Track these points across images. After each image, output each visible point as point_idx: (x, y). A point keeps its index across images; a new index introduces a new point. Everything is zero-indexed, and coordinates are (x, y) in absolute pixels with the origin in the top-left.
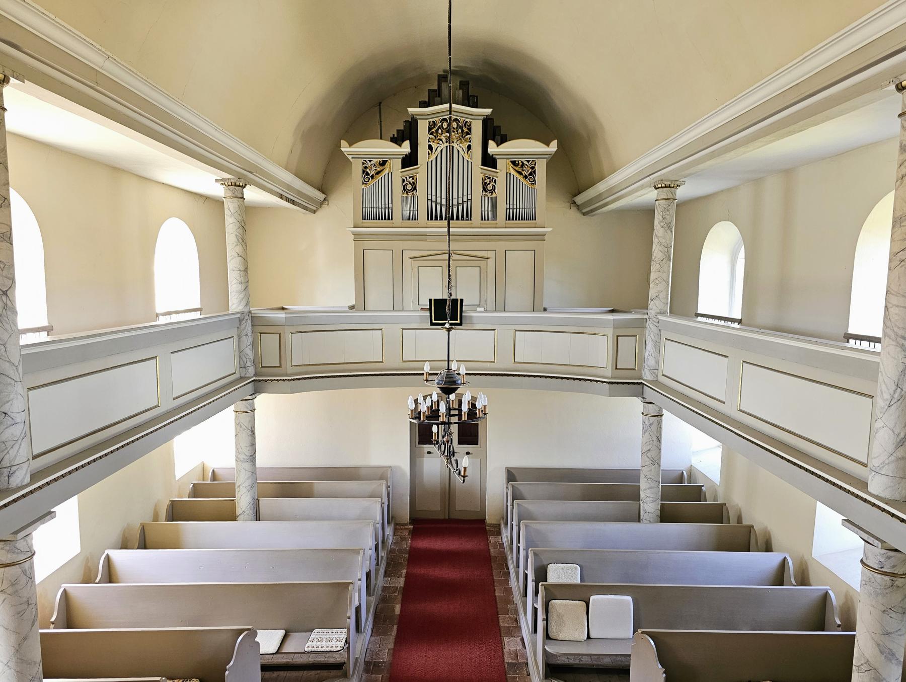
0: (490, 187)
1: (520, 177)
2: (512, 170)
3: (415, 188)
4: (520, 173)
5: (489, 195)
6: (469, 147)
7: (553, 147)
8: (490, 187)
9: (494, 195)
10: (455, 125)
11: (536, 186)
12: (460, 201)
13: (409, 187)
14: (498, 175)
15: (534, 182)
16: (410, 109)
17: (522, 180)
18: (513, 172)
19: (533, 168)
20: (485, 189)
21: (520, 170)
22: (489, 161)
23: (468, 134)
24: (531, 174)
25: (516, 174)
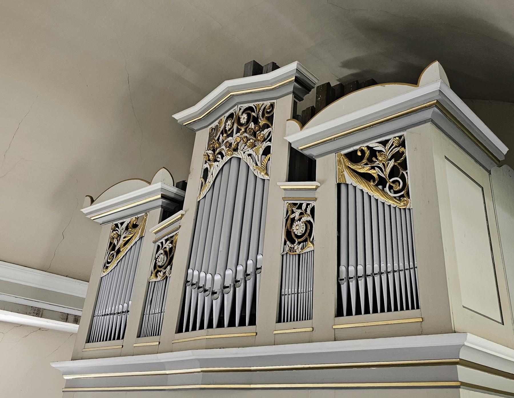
0: (299, 229)
1: (367, 188)
2: (346, 173)
3: (170, 262)
4: (367, 177)
5: (298, 248)
6: (267, 151)
7: (434, 79)
8: (299, 229)
9: (310, 247)
10: (244, 118)
11: (412, 203)
12: (240, 276)
13: (162, 259)
14: (317, 194)
15: (404, 193)
16: (177, 116)
17: (376, 195)
18: (350, 179)
19: (397, 156)
20: (290, 237)
21: (365, 170)
22: (302, 167)
23: (267, 126)
24: (394, 172)
25: (361, 186)
